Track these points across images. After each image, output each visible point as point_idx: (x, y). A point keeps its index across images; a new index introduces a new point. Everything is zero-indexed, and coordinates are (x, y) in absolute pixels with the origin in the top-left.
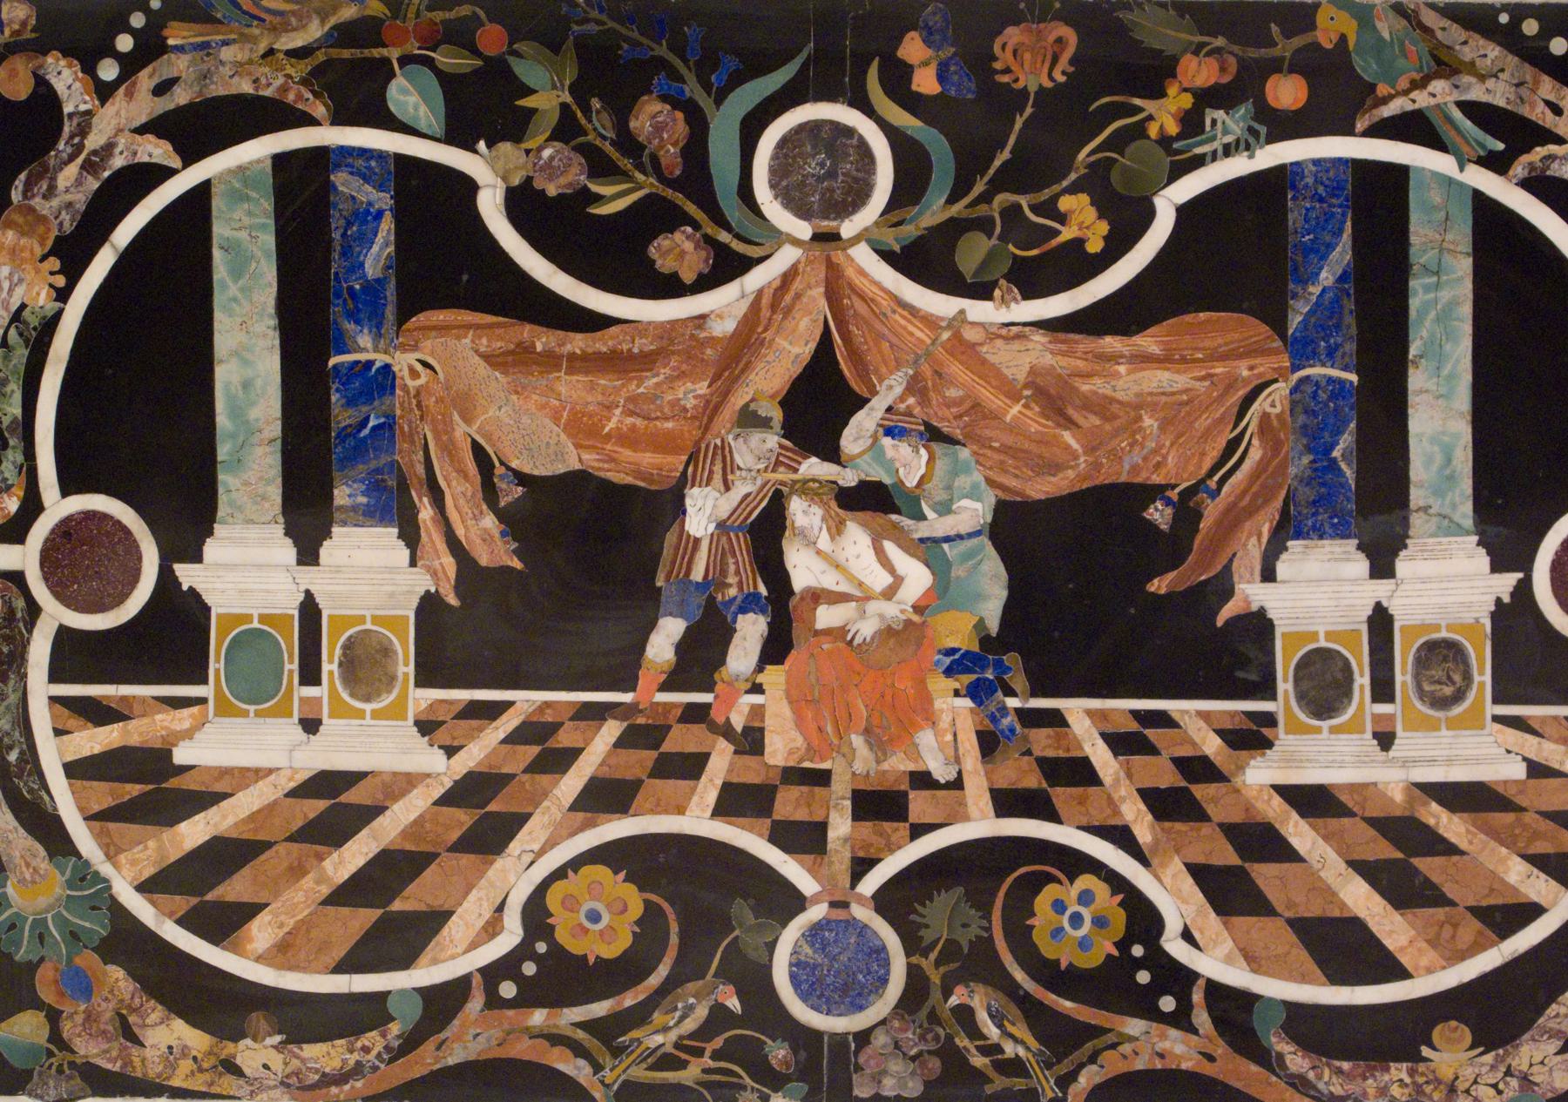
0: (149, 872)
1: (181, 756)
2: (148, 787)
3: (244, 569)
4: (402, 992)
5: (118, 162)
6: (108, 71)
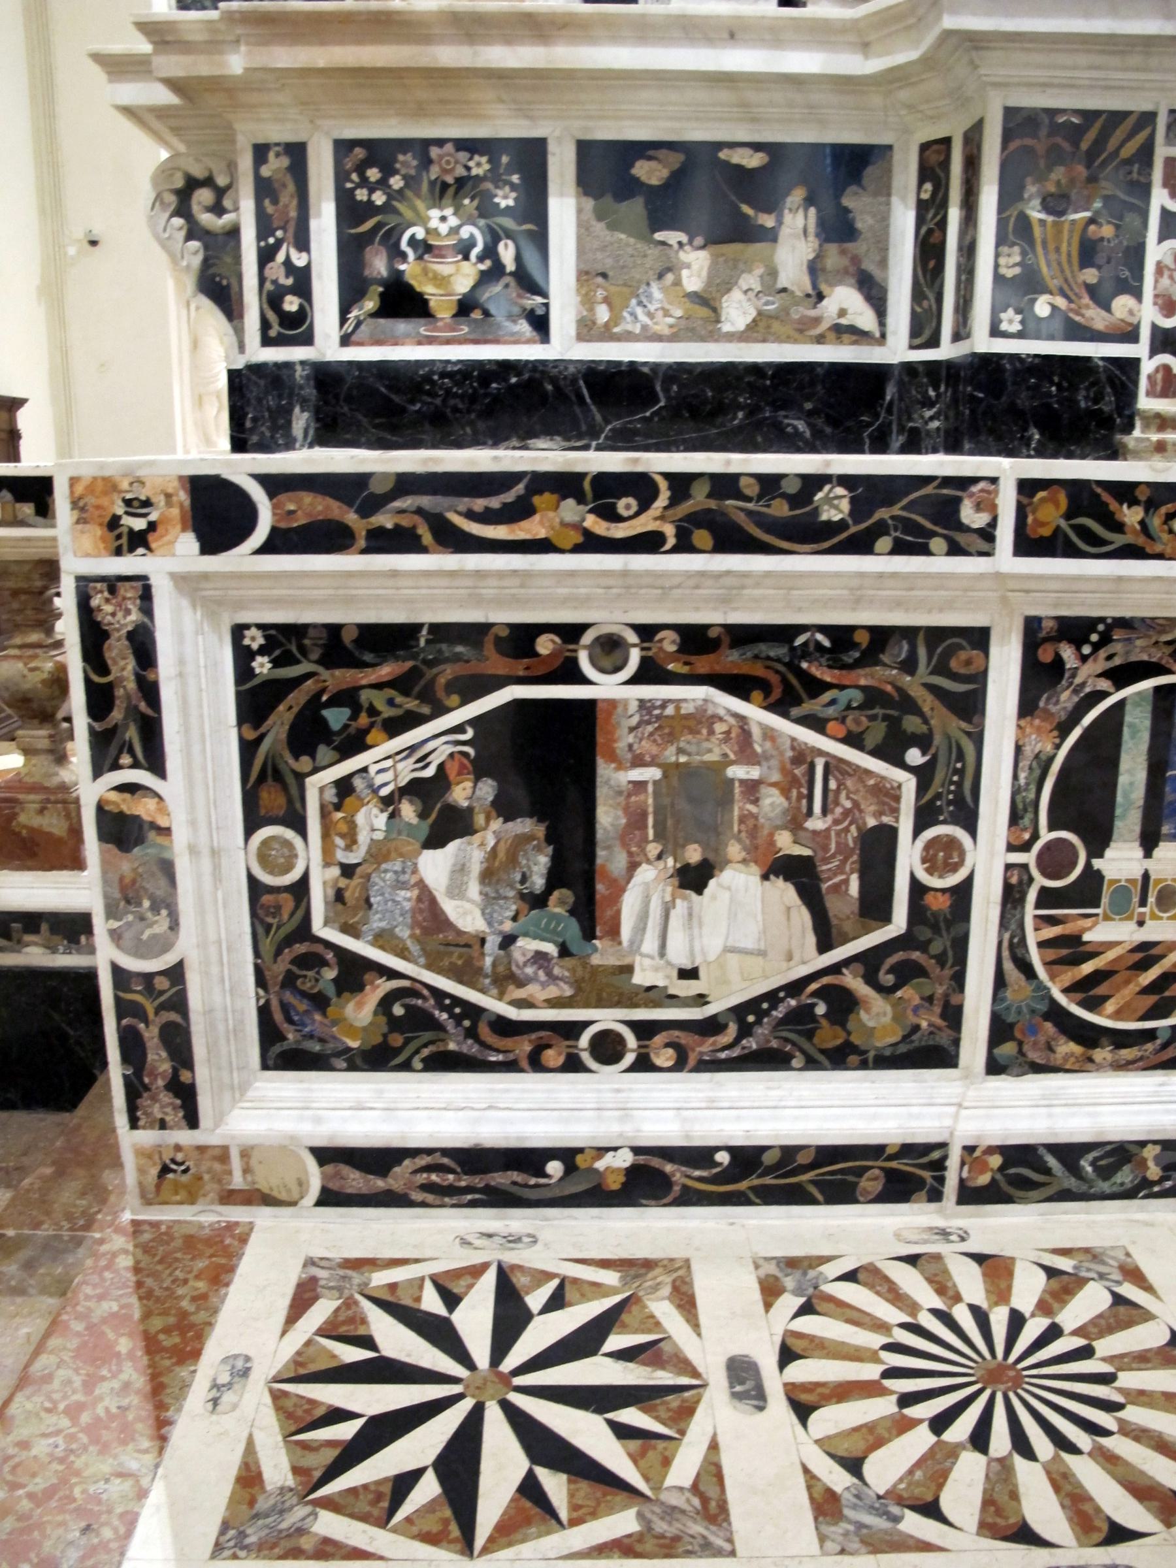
0: (1067, 984)
1: (1086, 937)
2: (1069, 949)
3: (1121, 861)
4: (1164, 1028)
5: (1088, 690)
6: (1086, 650)
